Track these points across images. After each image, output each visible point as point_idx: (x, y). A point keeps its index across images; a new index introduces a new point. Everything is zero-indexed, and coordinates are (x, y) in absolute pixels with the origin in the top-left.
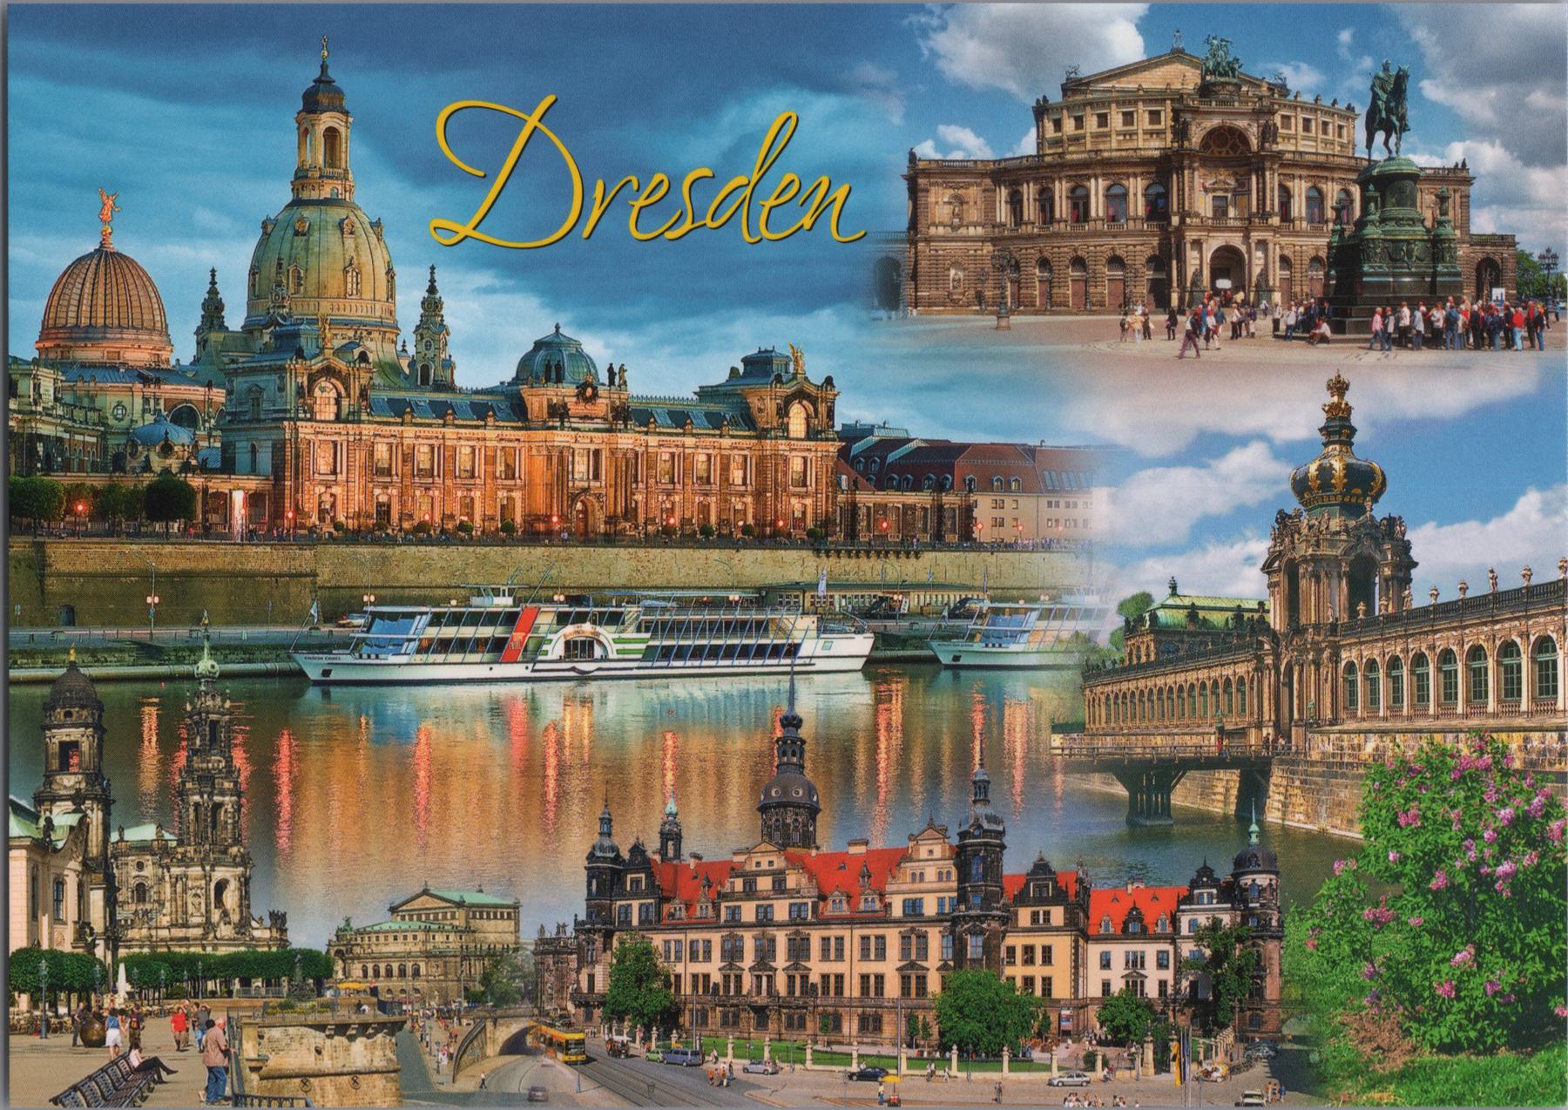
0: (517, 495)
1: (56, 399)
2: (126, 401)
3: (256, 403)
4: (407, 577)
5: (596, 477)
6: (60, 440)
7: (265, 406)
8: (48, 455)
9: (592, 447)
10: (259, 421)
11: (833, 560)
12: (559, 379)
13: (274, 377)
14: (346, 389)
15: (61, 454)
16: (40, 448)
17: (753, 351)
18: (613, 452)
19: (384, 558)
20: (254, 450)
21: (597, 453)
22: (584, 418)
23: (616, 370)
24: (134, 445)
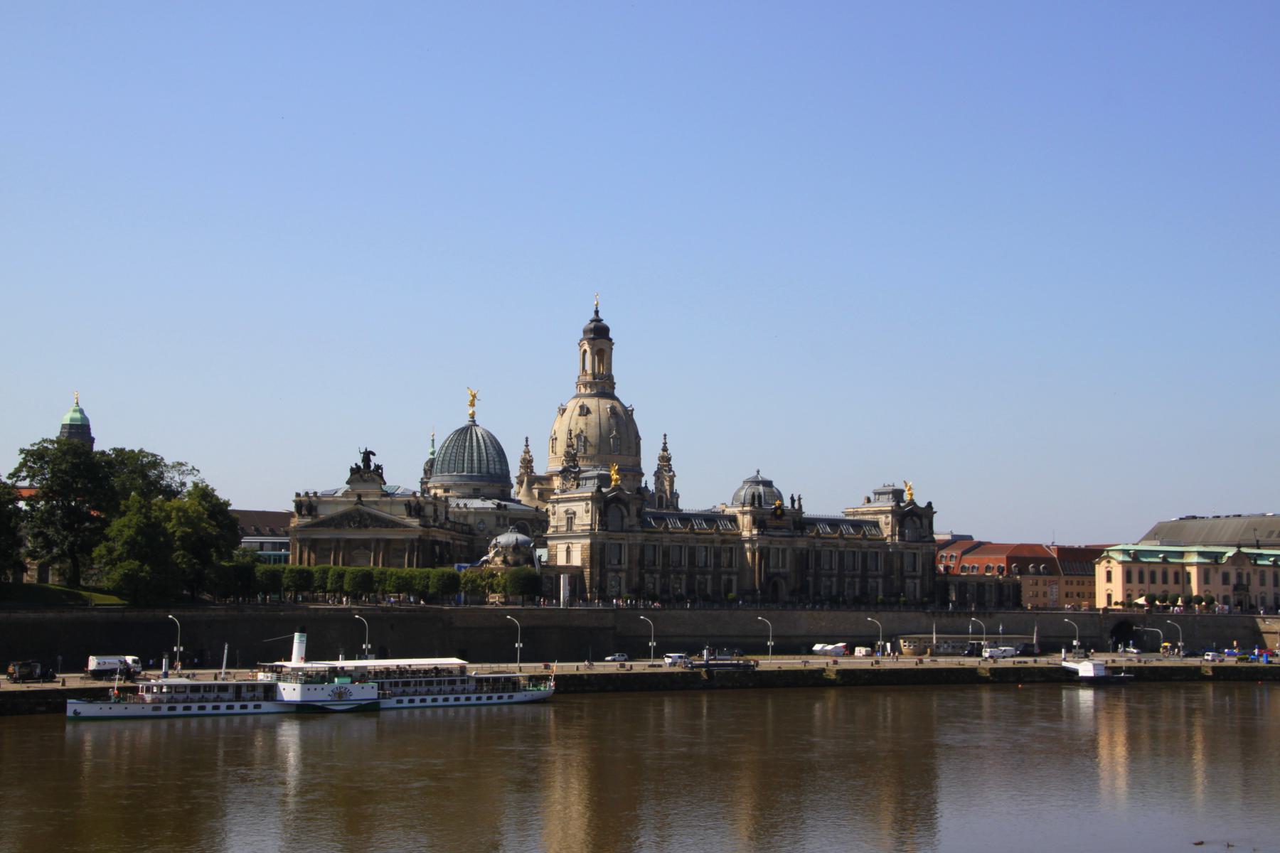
0: (734, 578)
1: (447, 518)
5: (784, 566)
6: (448, 544)
7: (577, 521)
9: (781, 547)
14: (628, 511)
16: (437, 549)
18: (794, 550)
20: (568, 551)
21: (784, 551)
22: (777, 528)
23: (796, 498)
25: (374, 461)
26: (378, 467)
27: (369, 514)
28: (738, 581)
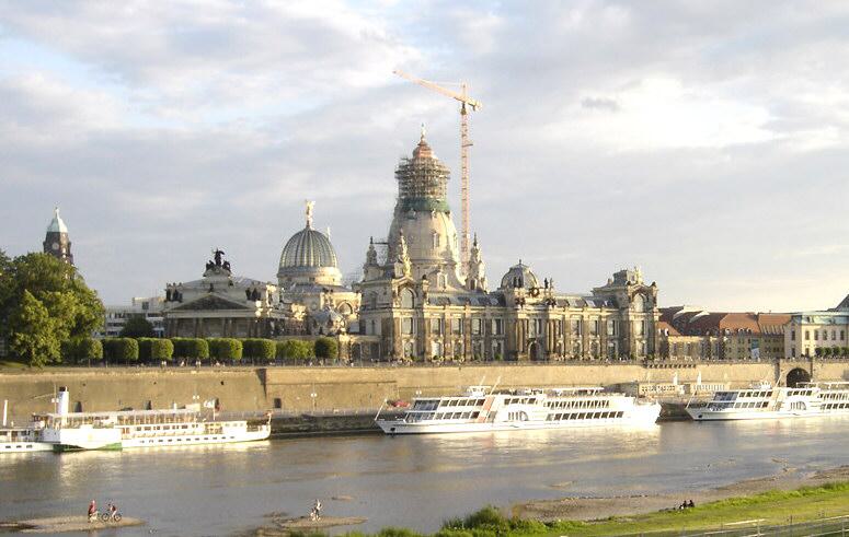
1: (281, 301)
3: (375, 300)
4: (444, 382)
6: (283, 320)
7: (379, 302)
12: (520, 286)
16: (272, 324)
19: (433, 374)
25: (223, 259)
26: (226, 263)
27: (219, 299)
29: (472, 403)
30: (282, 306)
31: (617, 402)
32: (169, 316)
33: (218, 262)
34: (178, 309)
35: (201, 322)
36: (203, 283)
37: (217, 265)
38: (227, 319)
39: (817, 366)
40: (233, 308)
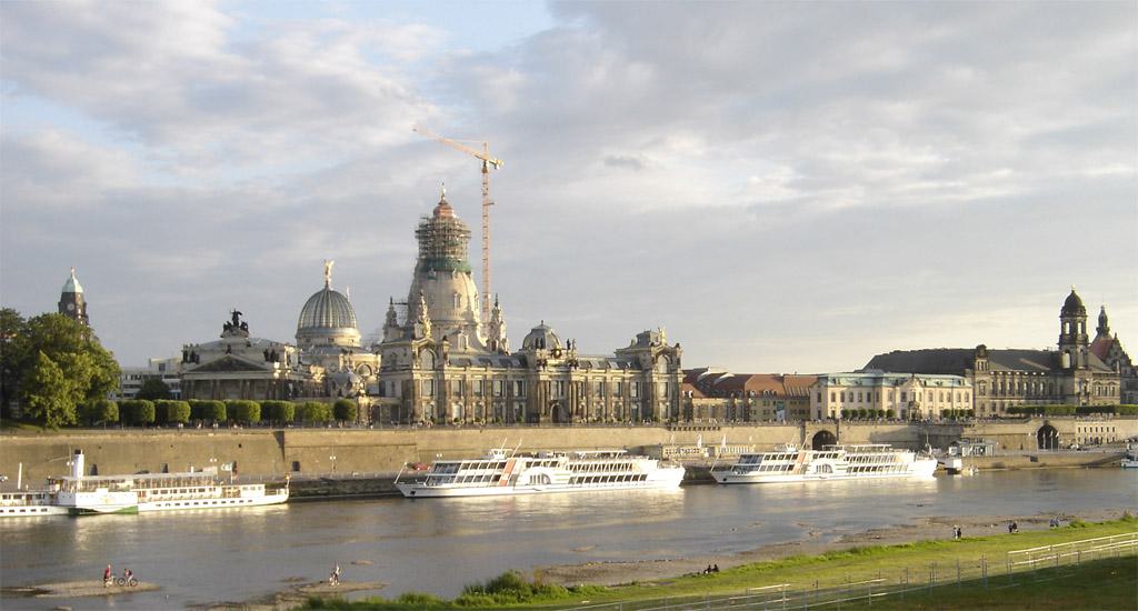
0: (523, 404)
1: (300, 363)
2: (336, 362)
3: (394, 362)
4: (466, 445)
6: (301, 382)
7: (399, 363)
8: (295, 389)
10: (395, 370)
11: (678, 432)
12: (542, 347)
13: (402, 350)
15: (302, 388)
16: (291, 386)
17: (642, 332)
19: (455, 437)
20: (393, 385)
23: (571, 342)
24: (334, 384)
25: (241, 319)
26: (244, 324)
27: (237, 361)
28: (527, 406)
29: (493, 466)
30: (301, 367)
31: (642, 465)
32: (186, 378)
33: (236, 323)
34: (198, 370)
35: (218, 384)
36: (221, 344)
37: (235, 326)
38: (245, 381)
39: (843, 428)
40: (251, 369)
